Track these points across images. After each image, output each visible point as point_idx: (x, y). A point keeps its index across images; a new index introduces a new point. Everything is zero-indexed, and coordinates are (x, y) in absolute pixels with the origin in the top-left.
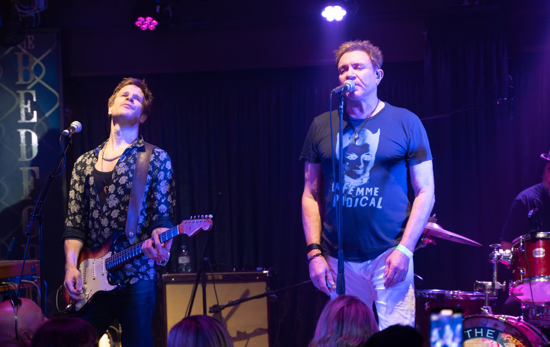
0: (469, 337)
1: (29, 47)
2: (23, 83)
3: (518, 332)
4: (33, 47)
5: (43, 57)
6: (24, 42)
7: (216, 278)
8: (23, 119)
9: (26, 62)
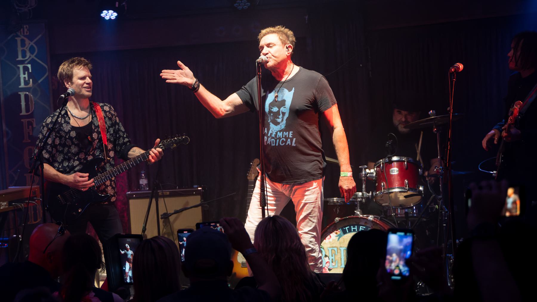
0: (348, 232)
1: (25, 34)
2: (22, 59)
3: (381, 227)
4: (28, 34)
5: (35, 40)
6: (22, 30)
7: (165, 194)
8: (22, 85)
9: (23, 44)
